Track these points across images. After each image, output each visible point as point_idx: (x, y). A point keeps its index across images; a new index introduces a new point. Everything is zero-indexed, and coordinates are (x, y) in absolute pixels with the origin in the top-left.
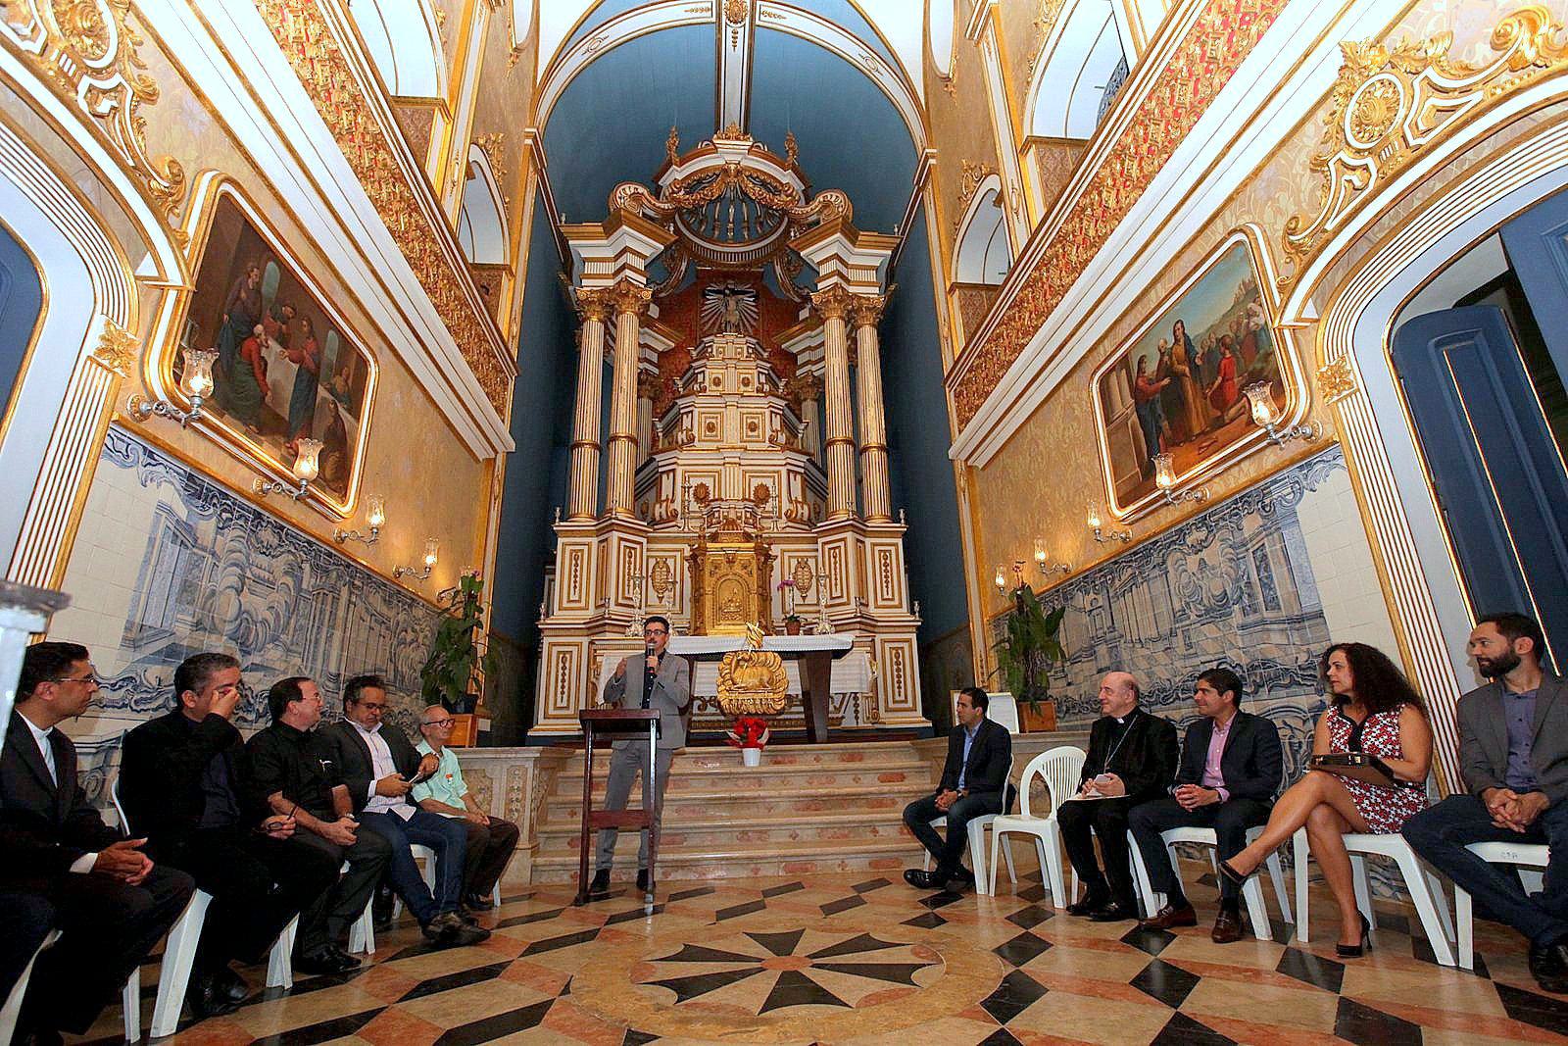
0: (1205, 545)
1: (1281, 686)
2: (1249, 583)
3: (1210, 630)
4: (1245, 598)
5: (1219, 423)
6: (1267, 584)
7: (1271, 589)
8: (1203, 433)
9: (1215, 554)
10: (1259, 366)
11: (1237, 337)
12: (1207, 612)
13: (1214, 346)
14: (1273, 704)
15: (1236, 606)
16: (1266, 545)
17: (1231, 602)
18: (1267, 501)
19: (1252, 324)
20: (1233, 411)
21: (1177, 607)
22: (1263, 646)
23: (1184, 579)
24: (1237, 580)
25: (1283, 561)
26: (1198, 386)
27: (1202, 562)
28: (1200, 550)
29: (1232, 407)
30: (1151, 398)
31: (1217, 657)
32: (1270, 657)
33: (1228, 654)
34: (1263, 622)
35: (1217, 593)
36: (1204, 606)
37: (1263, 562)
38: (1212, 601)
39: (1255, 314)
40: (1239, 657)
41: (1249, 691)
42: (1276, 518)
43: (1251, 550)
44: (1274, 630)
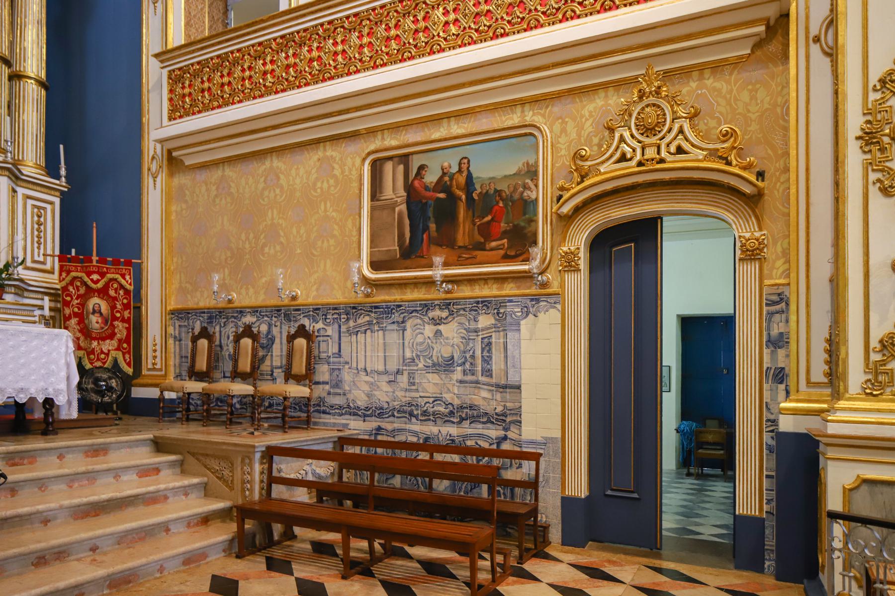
0: (445, 322)
1: (480, 422)
2: (473, 357)
3: (434, 378)
4: (467, 366)
5: (481, 247)
6: (487, 360)
7: (488, 364)
8: (465, 247)
9: (452, 331)
10: (522, 224)
11: (511, 196)
12: (434, 365)
13: (492, 192)
14: (470, 431)
15: (459, 368)
16: (493, 336)
17: (456, 364)
18: (502, 311)
19: (525, 194)
20: (494, 244)
21: (408, 354)
22: (474, 397)
23: (420, 339)
24: (465, 352)
25: (502, 350)
26: (470, 213)
27: (438, 333)
28: (439, 324)
29: (494, 241)
30: (424, 201)
31: (434, 395)
32: (476, 403)
33: (444, 395)
34: (477, 382)
35: (446, 355)
36: (433, 361)
37: (488, 346)
38: (440, 359)
39: (529, 189)
40: (453, 399)
41: (455, 420)
42: (504, 323)
43: (481, 337)
44: (484, 389)
